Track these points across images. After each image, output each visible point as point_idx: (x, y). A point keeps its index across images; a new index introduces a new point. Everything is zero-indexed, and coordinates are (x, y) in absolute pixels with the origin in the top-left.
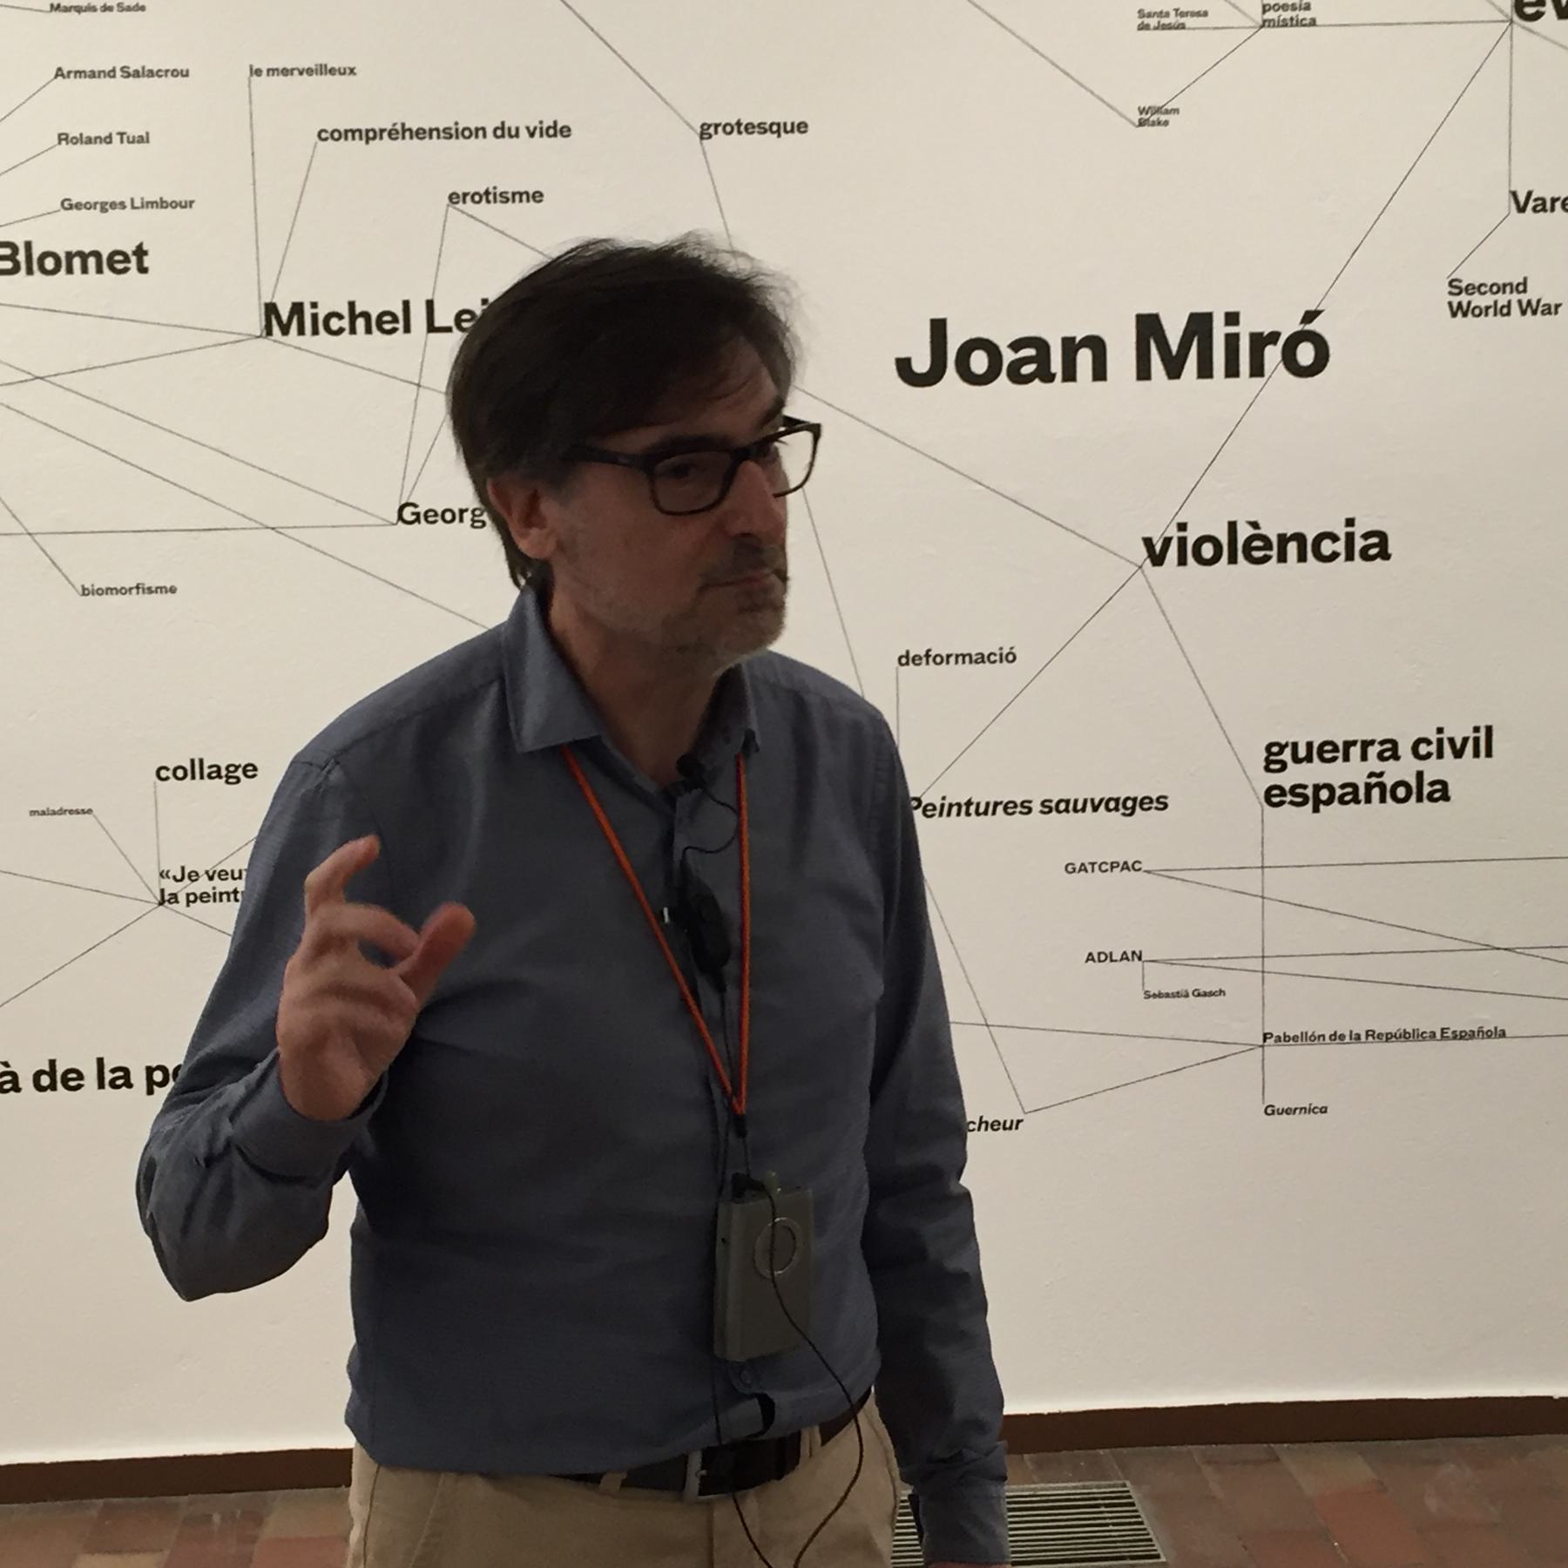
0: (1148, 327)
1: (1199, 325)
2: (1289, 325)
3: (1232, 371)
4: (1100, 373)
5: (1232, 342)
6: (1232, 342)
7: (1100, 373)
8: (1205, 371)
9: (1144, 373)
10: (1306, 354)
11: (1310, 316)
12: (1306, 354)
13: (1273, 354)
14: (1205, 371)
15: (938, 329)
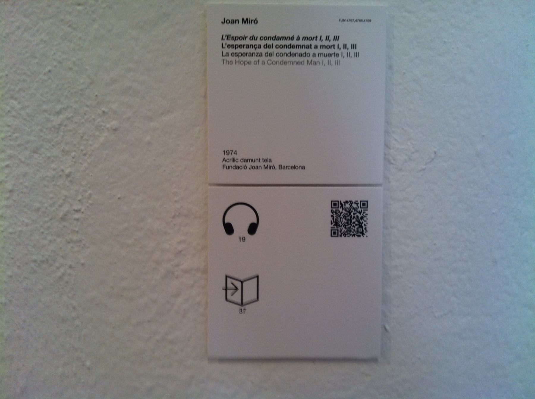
0: (243, 19)
1: (247, 19)
2: (254, 19)
3: (249, 23)
4: (238, 23)
5: (249, 21)
6: (250, 20)
7: (238, 23)
8: (247, 23)
9: (243, 23)
10: (256, 22)
11: (256, 19)
12: (256, 22)
13: (253, 22)
14: (247, 23)
15: (224, 19)
